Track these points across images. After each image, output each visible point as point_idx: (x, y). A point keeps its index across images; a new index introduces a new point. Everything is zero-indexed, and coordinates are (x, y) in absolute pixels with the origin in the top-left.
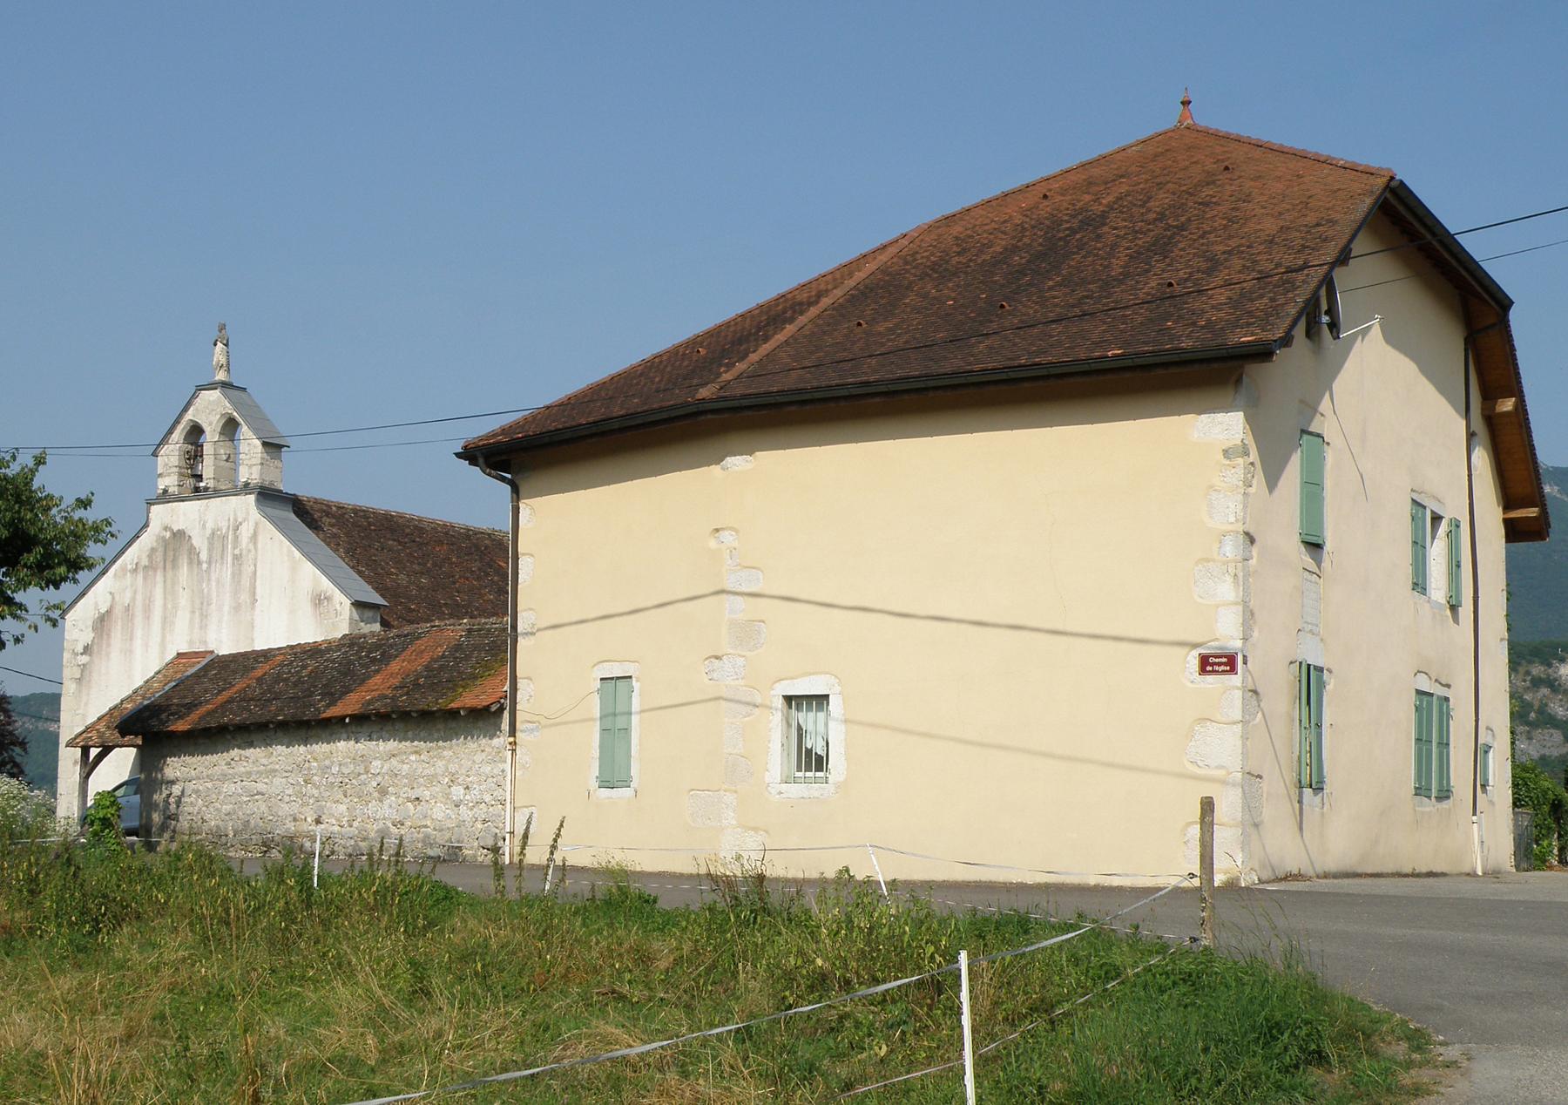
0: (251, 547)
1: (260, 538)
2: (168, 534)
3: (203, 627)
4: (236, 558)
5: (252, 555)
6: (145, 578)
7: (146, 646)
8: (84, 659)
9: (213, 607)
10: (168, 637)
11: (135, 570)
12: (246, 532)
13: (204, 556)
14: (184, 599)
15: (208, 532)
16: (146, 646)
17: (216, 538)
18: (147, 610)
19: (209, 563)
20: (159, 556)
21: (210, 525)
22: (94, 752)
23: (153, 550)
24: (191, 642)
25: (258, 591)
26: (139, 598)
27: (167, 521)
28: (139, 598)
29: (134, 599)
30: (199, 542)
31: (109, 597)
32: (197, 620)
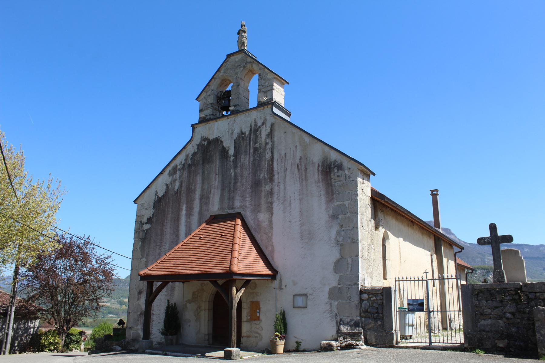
0: (269, 140)
1: (276, 133)
2: (206, 143)
3: (231, 199)
4: (256, 150)
5: (269, 146)
6: (189, 172)
7: (189, 214)
8: (148, 226)
9: (239, 184)
10: (204, 208)
11: (183, 169)
12: (264, 132)
13: (231, 152)
14: (216, 182)
15: (235, 136)
16: (189, 214)
17: (241, 140)
18: (190, 191)
19: (236, 155)
20: (199, 157)
21: (237, 131)
22: (157, 284)
23: (195, 154)
24: (221, 209)
25: (275, 169)
26: (184, 185)
27: (205, 135)
28: (184, 185)
29: (181, 186)
30: (229, 144)
31: (165, 187)
32: (226, 194)
